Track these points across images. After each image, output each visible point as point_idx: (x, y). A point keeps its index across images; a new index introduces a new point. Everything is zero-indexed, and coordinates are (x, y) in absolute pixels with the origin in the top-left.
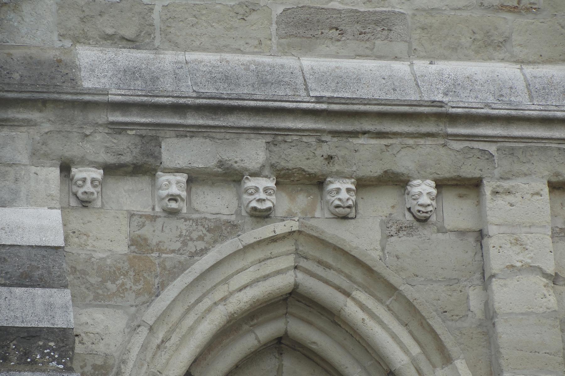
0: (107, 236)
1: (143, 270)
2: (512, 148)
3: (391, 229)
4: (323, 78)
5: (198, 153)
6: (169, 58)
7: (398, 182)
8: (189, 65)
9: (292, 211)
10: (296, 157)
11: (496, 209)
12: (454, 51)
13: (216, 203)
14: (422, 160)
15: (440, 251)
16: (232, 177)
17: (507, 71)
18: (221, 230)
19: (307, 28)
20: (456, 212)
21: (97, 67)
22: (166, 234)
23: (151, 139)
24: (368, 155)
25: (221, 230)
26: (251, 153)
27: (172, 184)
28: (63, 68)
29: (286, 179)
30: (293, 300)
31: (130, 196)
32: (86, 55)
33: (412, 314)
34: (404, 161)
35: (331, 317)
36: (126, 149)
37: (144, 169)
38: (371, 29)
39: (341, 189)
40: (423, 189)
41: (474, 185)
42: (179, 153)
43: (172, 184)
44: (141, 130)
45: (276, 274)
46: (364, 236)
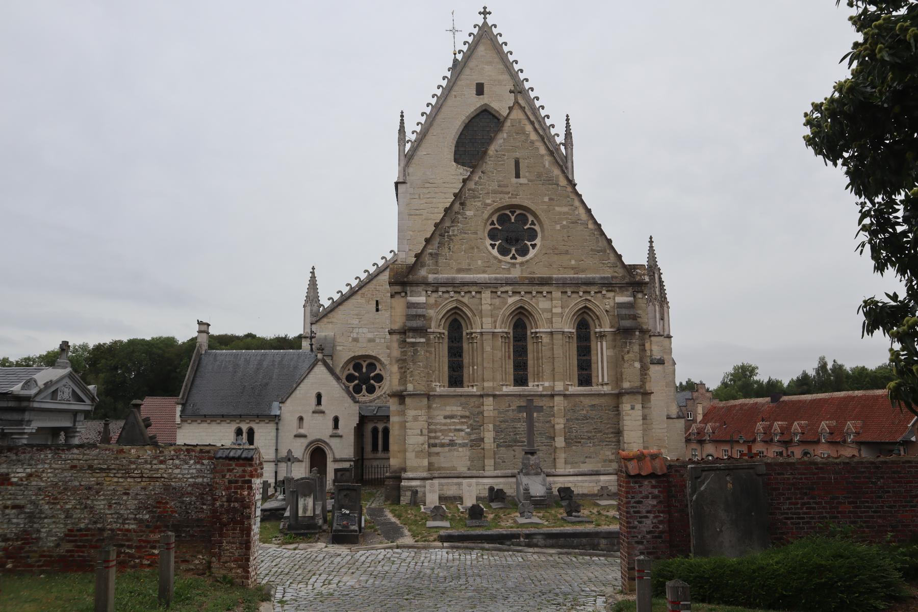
0: (432, 300)
1: (436, 304)
2: (487, 287)
3: (469, 298)
4: (462, 278)
5: (444, 289)
6: (441, 276)
7: (470, 292)
8: (443, 276)
9: (456, 296)
10: (456, 289)
11: (483, 295)
12: (479, 273)
13: (446, 295)
14: (473, 289)
15: (476, 301)
16: (448, 292)
17: (486, 276)
18: (447, 299)
19: (460, 271)
20: (478, 296)
21: (431, 277)
22: (439, 300)
23: (437, 287)
24: (466, 289)
25: (447, 299)
26: (450, 289)
27: (440, 293)
28: (426, 278)
29: (455, 292)
30: (456, 308)
31: (435, 295)
32: (430, 276)
33: (471, 310)
34: (471, 289)
35: (462, 311)
36: (434, 289)
37: (437, 291)
38: (468, 271)
39: (463, 293)
40: (474, 293)
41: (480, 292)
42: (441, 289)
43: (440, 293)
44: (435, 287)
45: (454, 305)
46: (465, 300)
